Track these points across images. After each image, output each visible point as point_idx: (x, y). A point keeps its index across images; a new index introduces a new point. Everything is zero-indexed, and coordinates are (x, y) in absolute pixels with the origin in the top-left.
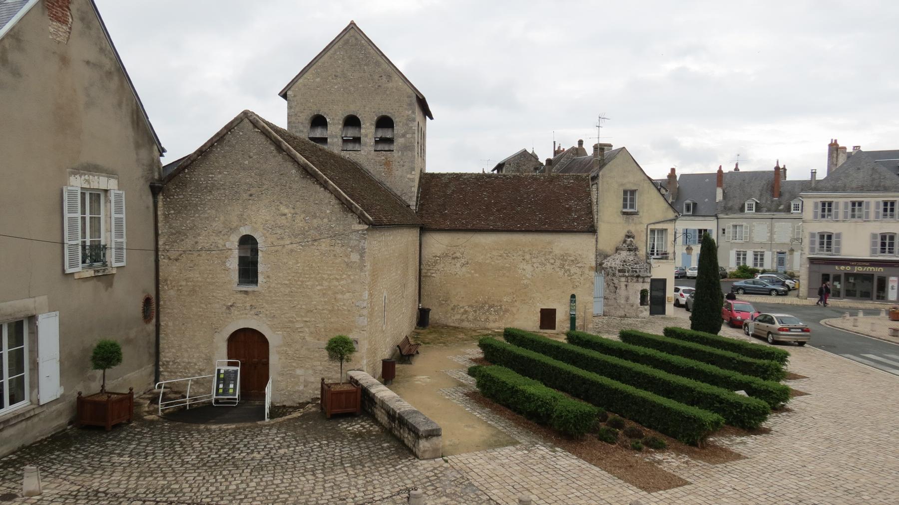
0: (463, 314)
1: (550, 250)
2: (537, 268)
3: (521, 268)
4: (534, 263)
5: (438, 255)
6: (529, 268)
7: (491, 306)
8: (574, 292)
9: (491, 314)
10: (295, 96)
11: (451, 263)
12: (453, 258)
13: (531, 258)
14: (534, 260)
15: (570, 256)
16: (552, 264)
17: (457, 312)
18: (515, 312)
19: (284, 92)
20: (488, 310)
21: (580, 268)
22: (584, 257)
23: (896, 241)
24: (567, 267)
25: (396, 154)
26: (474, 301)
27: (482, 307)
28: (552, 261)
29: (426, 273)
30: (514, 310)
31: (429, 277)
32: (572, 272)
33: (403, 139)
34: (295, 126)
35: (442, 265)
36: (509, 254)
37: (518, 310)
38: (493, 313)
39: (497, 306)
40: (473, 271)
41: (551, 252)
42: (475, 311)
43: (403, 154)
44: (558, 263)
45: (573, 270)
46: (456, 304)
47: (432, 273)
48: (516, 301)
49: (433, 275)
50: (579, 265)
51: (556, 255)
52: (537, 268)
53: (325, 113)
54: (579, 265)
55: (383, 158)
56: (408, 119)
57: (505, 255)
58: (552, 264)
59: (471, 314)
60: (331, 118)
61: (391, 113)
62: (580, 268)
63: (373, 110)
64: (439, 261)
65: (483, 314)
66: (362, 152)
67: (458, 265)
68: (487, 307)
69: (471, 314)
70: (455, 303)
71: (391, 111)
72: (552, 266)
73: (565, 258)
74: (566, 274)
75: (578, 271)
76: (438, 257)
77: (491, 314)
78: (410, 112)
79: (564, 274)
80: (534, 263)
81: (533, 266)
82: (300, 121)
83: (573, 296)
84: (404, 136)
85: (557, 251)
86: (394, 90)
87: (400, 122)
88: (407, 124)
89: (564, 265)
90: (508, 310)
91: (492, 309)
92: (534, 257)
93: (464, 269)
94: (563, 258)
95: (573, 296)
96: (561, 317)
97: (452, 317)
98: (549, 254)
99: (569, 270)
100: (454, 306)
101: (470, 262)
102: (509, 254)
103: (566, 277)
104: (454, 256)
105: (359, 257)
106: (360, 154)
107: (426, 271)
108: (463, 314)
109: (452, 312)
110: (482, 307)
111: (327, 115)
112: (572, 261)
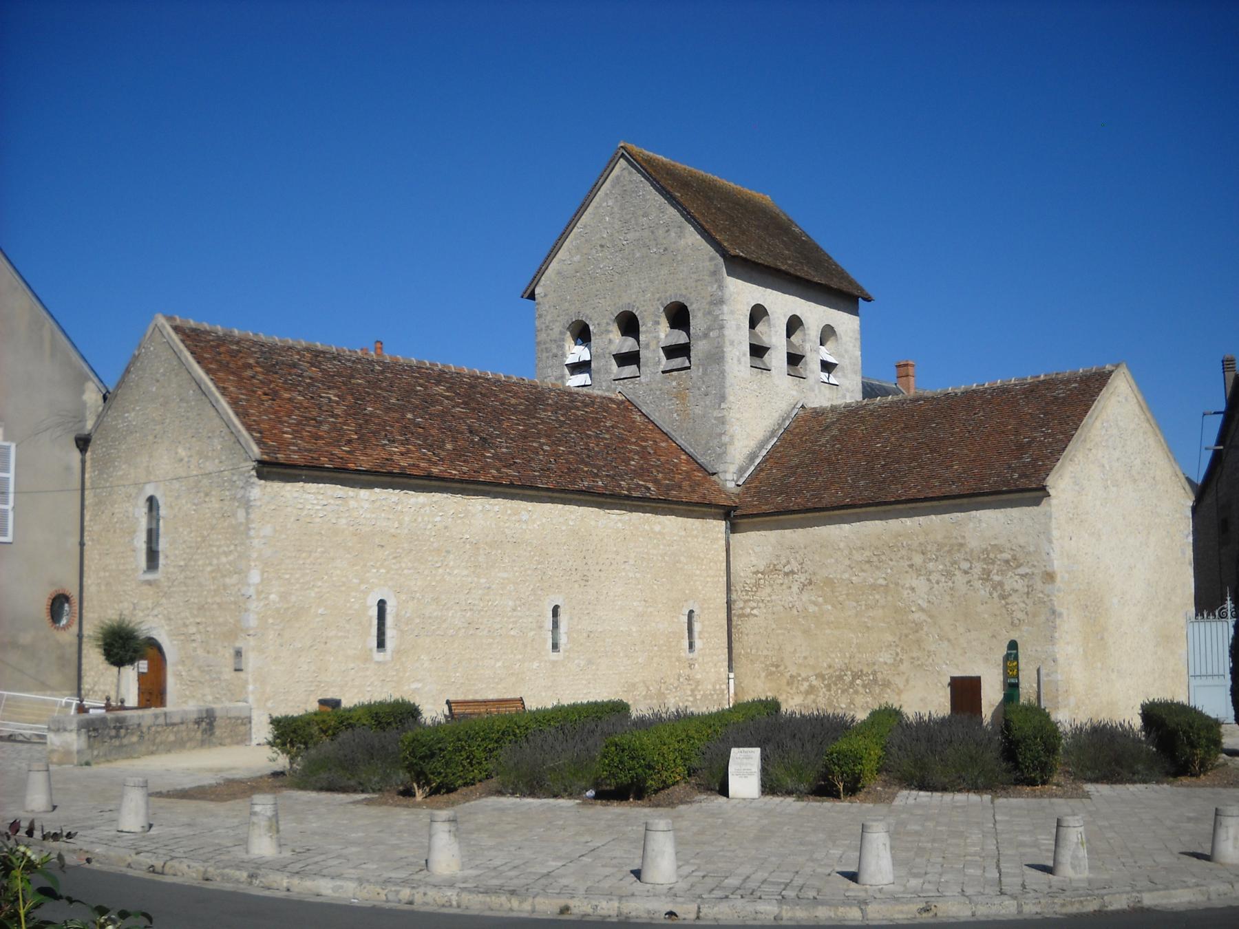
0: (808, 693)
1: (961, 541)
2: (938, 583)
3: (907, 585)
4: (930, 573)
5: (762, 568)
6: (921, 584)
7: (856, 676)
8: (1014, 636)
9: (856, 692)
10: (545, 295)
11: (782, 584)
12: (786, 574)
13: (924, 561)
14: (931, 565)
15: (1001, 552)
16: (966, 572)
17: (797, 688)
18: (901, 686)
19: (529, 291)
20: (852, 683)
21: (1023, 576)
22: (1032, 549)
23: (521, 293)
24: (997, 578)
25: (696, 372)
26: (825, 665)
27: (840, 678)
28: (965, 565)
29: (741, 608)
30: (899, 681)
31: (748, 616)
32: (1007, 587)
33: (704, 342)
34: (546, 349)
35: (768, 590)
36: (883, 557)
37: (907, 681)
38: (861, 690)
39: (867, 675)
40: (820, 600)
41: (961, 545)
42: (828, 687)
43: (705, 373)
44: (978, 568)
45: (1012, 582)
46: (794, 674)
47: (752, 609)
48: (901, 661)
49: (755, 612)
50: (1021, 571)
51: (972, 551)
52: (938, 583)
53: (587, 317)
54: (1021, 571)
55: (674, 384)
56: (711, 303)
57: (875, 559)
58: (966, 572)
59: (821, 694)
60: (596, 322)
61: (684, 296)
62: (1023, 576)
63: (658, 296)
64: (762, 581)
65: (843, 692)
66: (643, 379)
67: (795, 589)
68: (848, 679)
69: (821, 694)
70: (793, 670)
71: (684, 292)
72: (967, 578)
73: (992, 556)
74: (995, 595)
75: (1020, 585)
76: (762, 573)
77: (856, 692)
78: (715, 286)
79: (991, 594)
80: (930, 573)
81: (929, 580)
82: (554, 337)
83: (1013, 645)
84: (706, 336)
85: (973, 543)
86: (688, 251)
87: (699, 310)
88: (710, 313)
89: (989, 573)
90: (889, 682)
91: (858, 682)
92: (930, 560)
93: (805, 597)
94: (988, 556)
95: (1013, 645)
96: (991, 696)
97: (790, 700)
98: (959, 551)
99: (1001, 584)
100: (791, 676)
101: (814, 579)
102: (883, 557)
103: (996, 599)
104: (787, 569)
105: (245, 514)
106: (640, 383)
107: (741, 604)
108: (808, 693)
109: (788, 689)
110: (840, 678)
111: (591, 319)
112: (1007, 562)
